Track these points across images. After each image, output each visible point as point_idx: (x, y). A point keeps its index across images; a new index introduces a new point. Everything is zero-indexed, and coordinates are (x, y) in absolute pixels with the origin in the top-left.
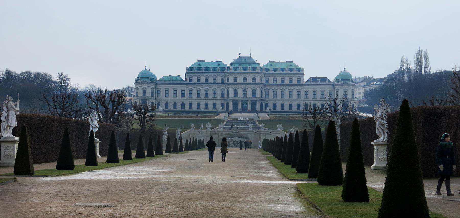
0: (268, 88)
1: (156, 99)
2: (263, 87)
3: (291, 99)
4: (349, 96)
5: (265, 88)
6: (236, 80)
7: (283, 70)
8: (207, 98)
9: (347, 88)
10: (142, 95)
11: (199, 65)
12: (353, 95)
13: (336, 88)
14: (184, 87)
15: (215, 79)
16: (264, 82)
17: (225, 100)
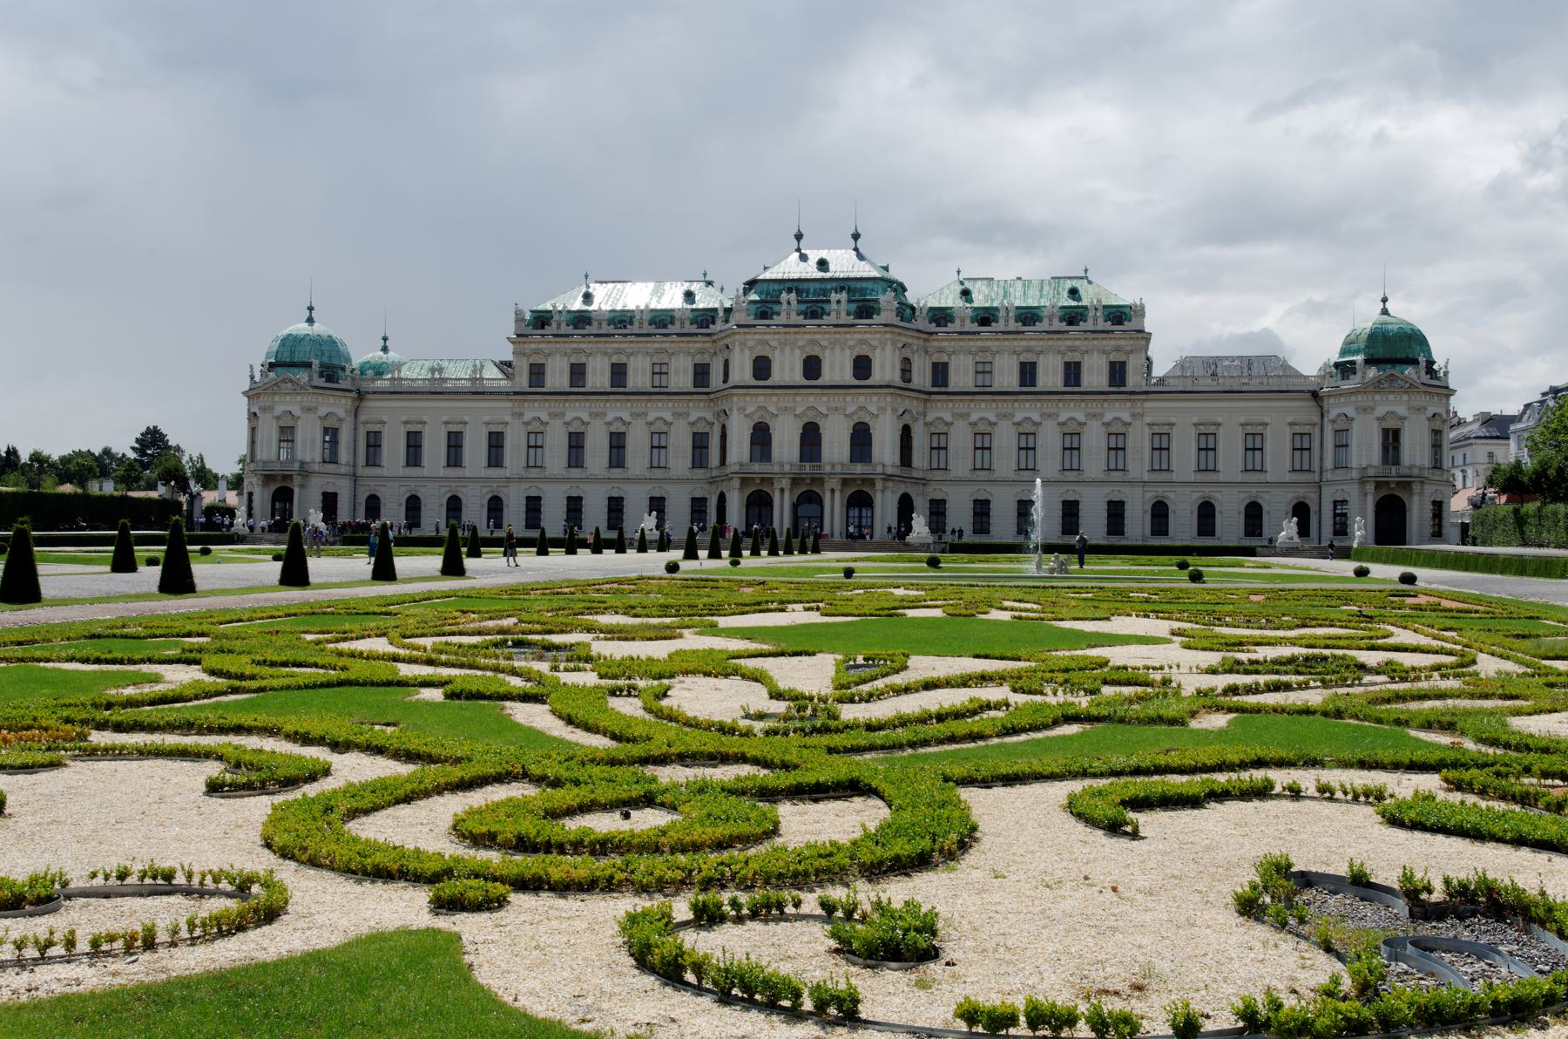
0: (947, 417)
1: (355, 477)
2: (915, 406)
3: (1071, 476)
4: (1415, 451)
5: (930, 418)
6: (762, 367)
7: (1028, 316)
8: (616, 472)
9: (1402, 410)
10: (274, 458)
12: (1437, 446)
14: (500, 412)
15: (659, 371)
16: (922, 377)
17: (712, 481)
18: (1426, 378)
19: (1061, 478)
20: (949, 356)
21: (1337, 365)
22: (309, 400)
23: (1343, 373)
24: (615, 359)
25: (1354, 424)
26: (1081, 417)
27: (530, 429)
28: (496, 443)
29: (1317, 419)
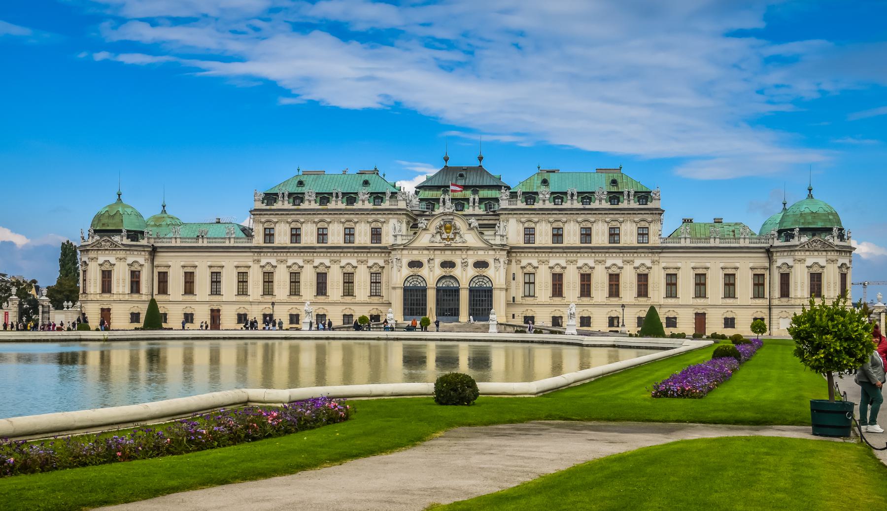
0: (535, 264)
7: (586, 197)
9: (822, 261)
11: (301, 183)
13: (780, 260)
14: (246, 259)
18: (837, 242)
19: (608, 302)
20: (536, 223)
21: (780, 232)
22: (121, 254)
23: (786, 235)
24: (319, 225)
25: (793, 270)
26: (620, 264)
27: (265, 270)
28: (243, 280)
29: (767, 265)
